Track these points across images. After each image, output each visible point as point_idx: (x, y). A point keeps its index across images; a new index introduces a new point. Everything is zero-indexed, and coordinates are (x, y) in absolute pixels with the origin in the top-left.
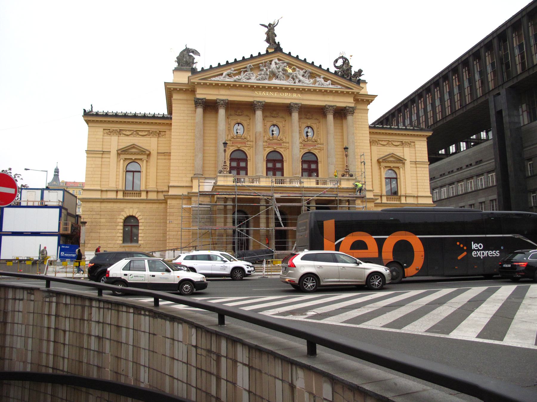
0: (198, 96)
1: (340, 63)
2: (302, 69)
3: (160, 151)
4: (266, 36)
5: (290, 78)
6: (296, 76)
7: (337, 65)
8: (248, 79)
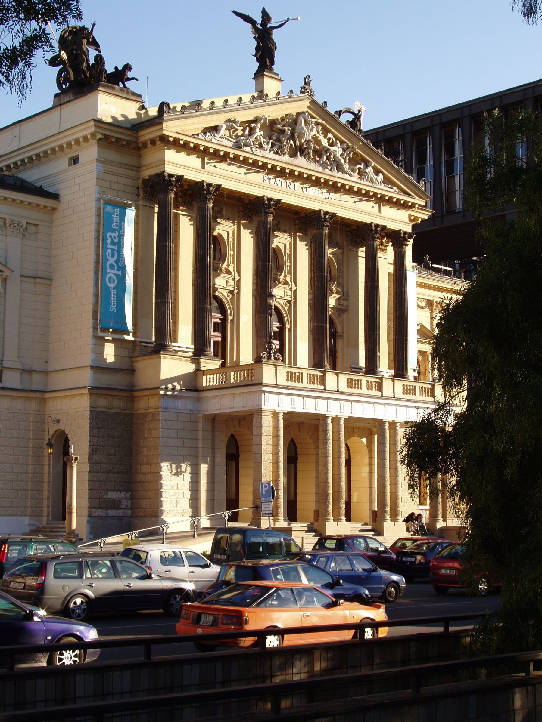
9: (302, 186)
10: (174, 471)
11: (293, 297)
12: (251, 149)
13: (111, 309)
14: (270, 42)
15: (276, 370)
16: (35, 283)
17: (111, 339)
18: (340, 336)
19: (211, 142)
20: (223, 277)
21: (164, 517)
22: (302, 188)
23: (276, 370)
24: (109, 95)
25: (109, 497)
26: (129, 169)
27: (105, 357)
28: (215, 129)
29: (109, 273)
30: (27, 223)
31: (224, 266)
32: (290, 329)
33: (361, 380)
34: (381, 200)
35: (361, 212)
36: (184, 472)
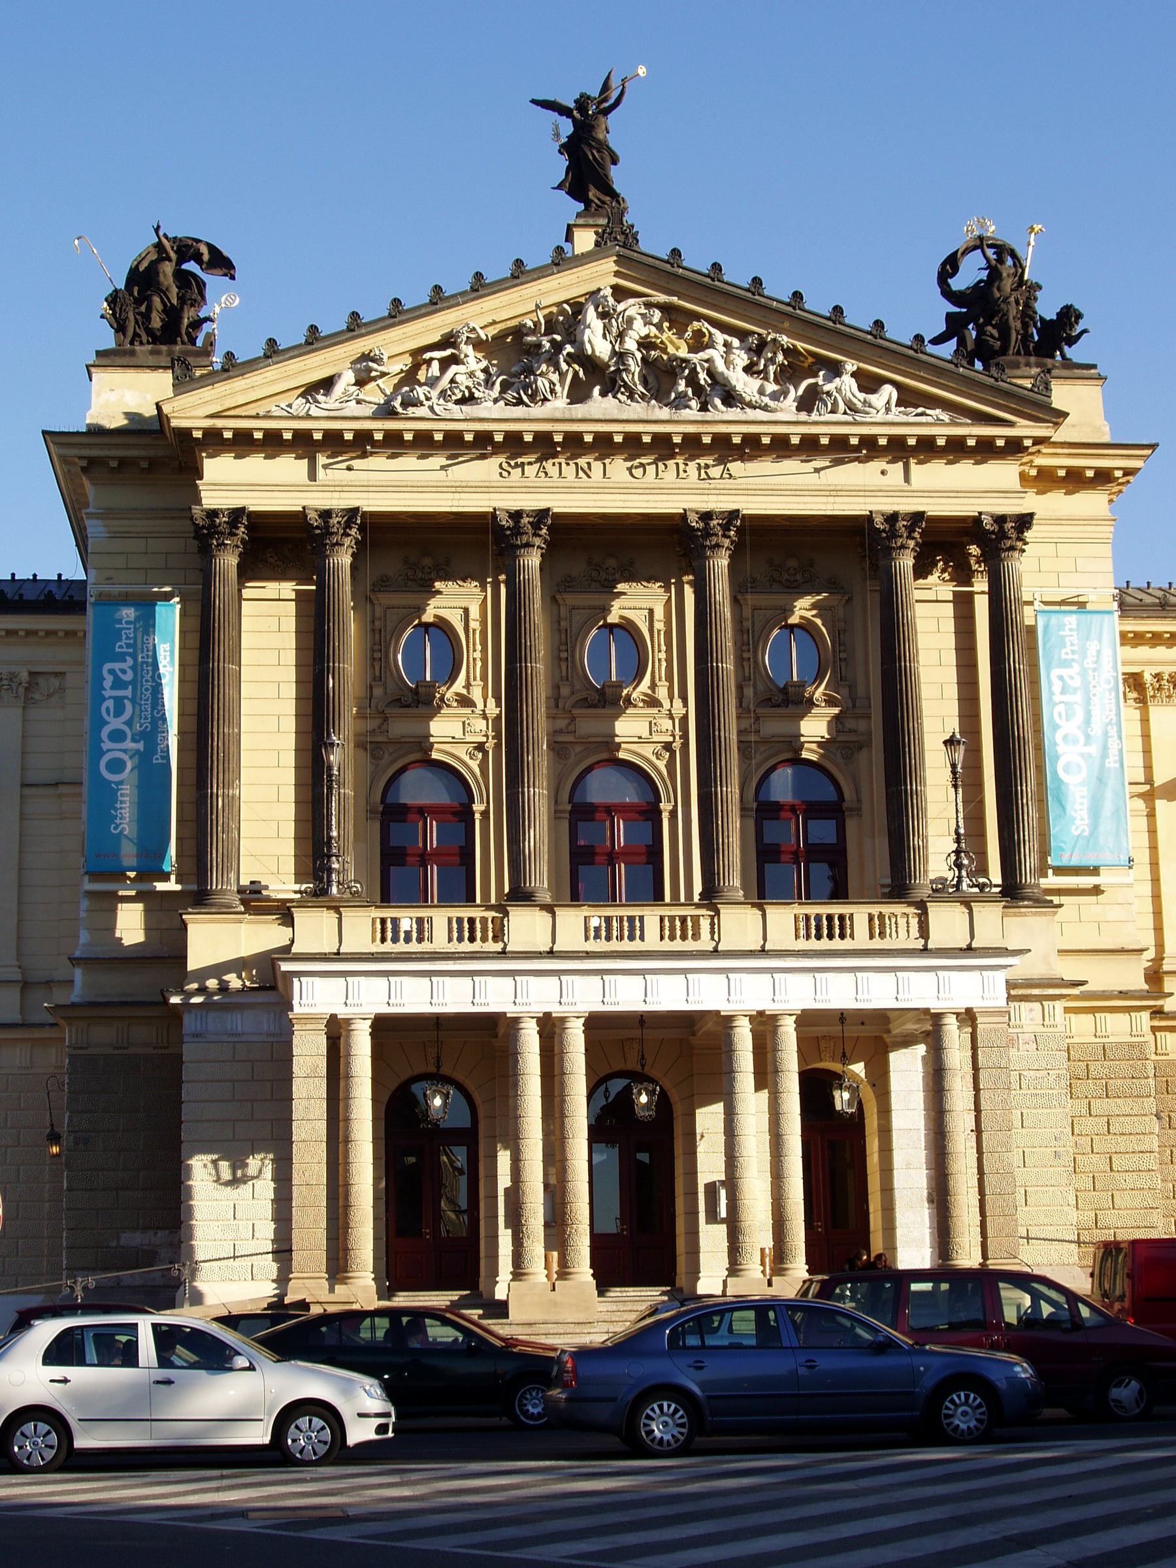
0: (211, 499)
1: (970, 273)
2: (742, 335)
3: (32, 777)
4: (563, 162)
5: (682, 386)
6: (711, 373)
7: (959, 283)
8: (462, 401)
9: (629, 464)
10: (226, 1175)
11: (490, 733)
12: (431, 408)
13: (115, 829)
14: (591, 147)
15: (340, 919)
16: (60, 796)
17: (133, 893)
18: (851, 810)
19: (308, 417)
20: (448, 716)
21: (199, 1284)
22: (630, 469)
23: (340, 919)
24: (120, 370)
25: (121, 1243)
26: (173, 518)
27: (118, 935)
28: (327, 384)
29: (108, 751)
30: (31, 674)
31: (459, 686)
32: (673, 814)
33: (641, 918)
34: (898, 449)
35: (835, 492)
36: (253, 1178)
